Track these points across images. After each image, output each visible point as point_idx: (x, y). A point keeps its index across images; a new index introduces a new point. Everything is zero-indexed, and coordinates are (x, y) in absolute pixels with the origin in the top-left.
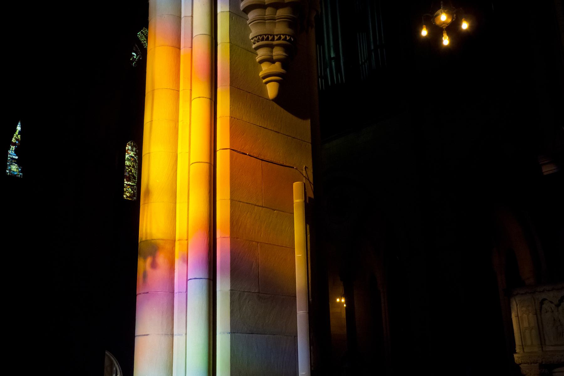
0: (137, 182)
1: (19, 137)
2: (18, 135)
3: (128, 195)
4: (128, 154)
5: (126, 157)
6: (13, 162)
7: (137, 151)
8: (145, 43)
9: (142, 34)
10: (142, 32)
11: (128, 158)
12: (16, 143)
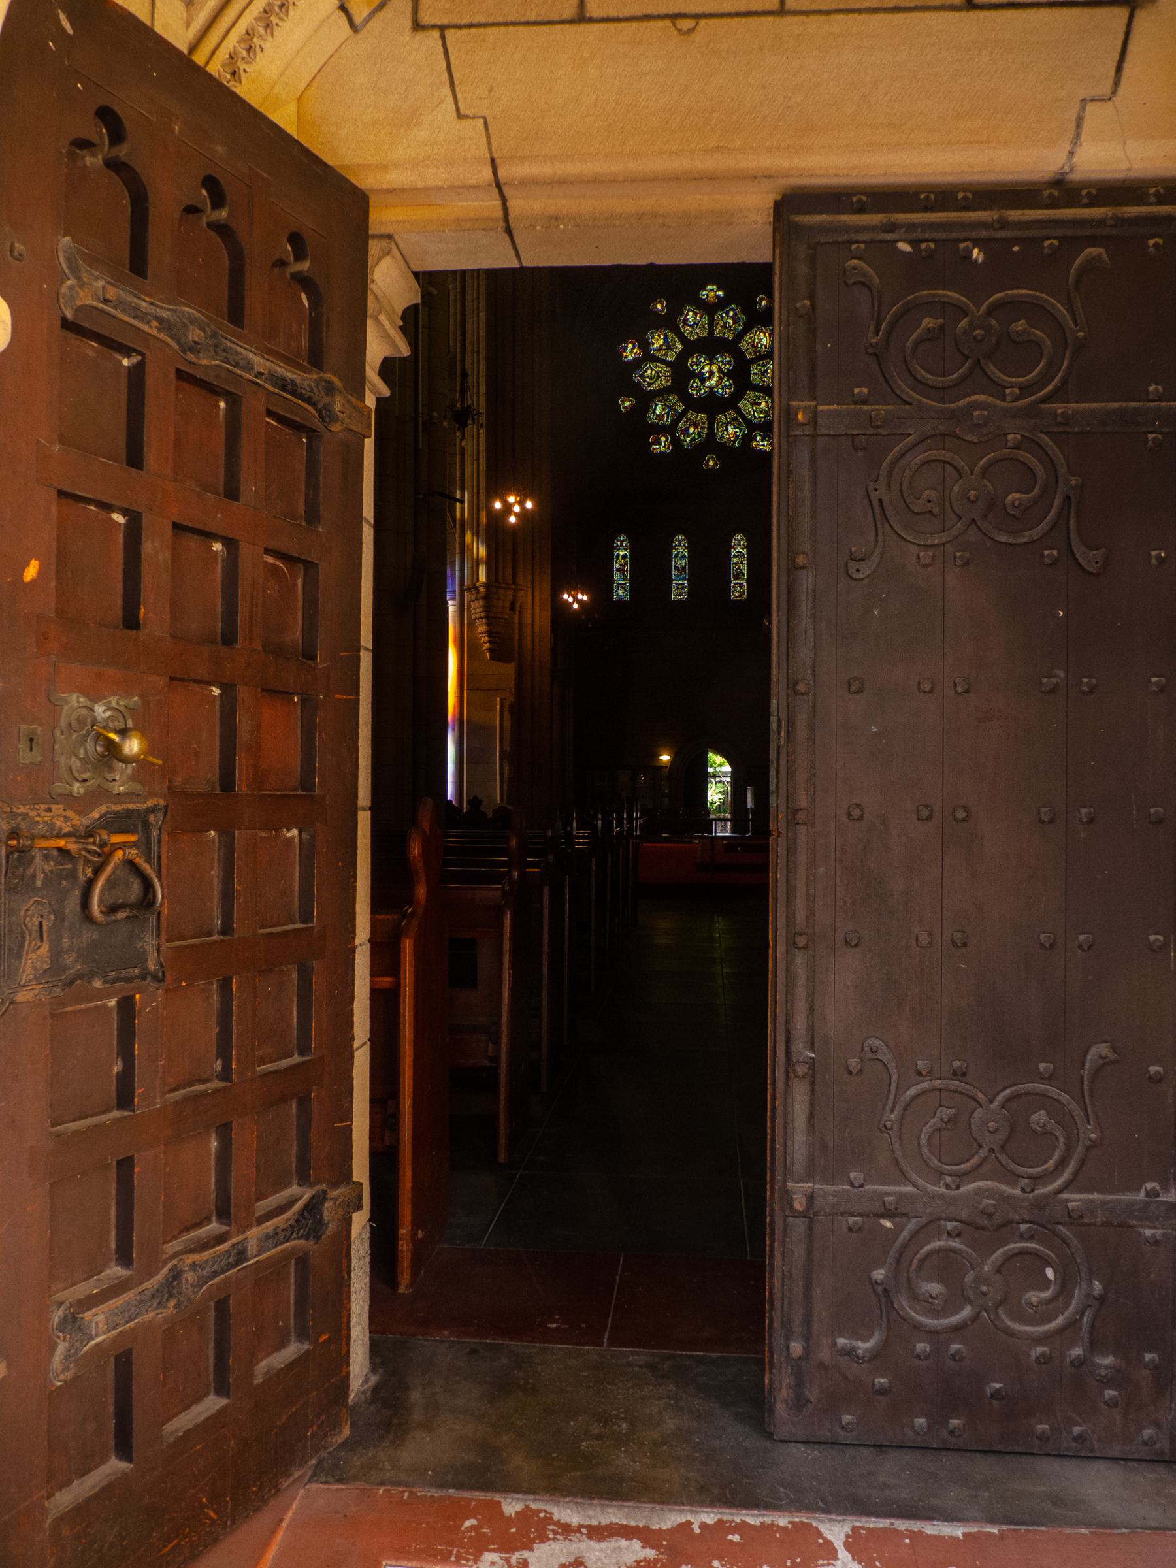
3: (737, 594)
10: (746, 399)
11: (734, 555)
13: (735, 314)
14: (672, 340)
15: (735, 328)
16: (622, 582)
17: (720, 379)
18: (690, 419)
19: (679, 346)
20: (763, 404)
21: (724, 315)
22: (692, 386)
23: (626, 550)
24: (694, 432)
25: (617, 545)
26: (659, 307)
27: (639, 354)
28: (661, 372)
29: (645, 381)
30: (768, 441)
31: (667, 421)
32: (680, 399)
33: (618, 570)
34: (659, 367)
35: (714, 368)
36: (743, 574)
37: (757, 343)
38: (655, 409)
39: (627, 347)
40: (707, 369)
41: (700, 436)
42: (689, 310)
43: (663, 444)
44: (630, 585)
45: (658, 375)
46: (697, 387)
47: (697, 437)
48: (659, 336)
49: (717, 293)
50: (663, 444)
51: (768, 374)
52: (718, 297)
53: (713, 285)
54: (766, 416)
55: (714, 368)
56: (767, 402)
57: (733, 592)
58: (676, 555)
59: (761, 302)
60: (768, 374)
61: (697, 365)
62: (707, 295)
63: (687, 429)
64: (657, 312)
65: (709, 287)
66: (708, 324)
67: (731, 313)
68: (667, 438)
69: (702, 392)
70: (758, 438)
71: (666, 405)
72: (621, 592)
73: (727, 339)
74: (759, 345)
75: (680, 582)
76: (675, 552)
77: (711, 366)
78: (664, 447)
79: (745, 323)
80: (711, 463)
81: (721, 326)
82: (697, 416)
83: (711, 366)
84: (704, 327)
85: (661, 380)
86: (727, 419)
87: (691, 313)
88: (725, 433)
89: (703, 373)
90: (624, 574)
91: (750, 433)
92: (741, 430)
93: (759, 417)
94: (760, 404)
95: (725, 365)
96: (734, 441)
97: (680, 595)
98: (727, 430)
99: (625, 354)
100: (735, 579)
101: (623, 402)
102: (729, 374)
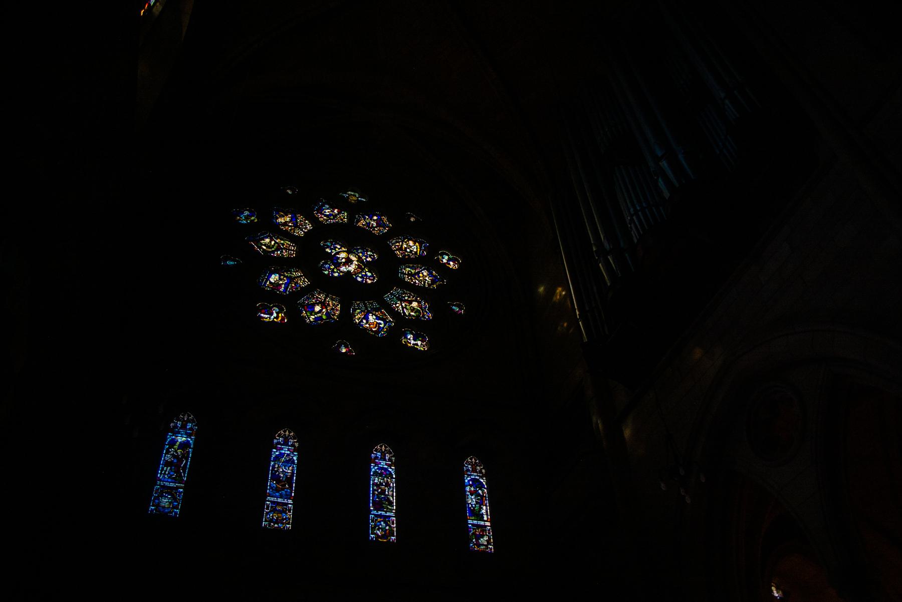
0: (395, 510)
5: (373, 470)
6: (166, 493)
7: (393, 459)
8: (398, 307)
10: (392, 294)
11: (376, 474)
12: (172, 461)
14: (300, 221)
16: (172, 485)
19: (309, 227)
20: (415, 304)
23: (189, 435)
24: (320, 312)
28: (283, 244)
29: (260, 248)
30: (422, 341)
33: (167, 464)
36: (391, 503)
37: (406, 248)
43: (275, 315)
44: (185, 492)
47: (324, 317)
56: (419, 302)
57: (373, 529)
58: (277, 458)
60: (419, 277)
63: (313, 305)
65: (349, 193)
70: (410, 336)
72: (165, 502)
74: (408, 250)
75: (280, 500)
76: (275, 453)
78: (277, 317)
88: (364, 321)
90: (177, 472)
94: (410, 302)
95: (367, 257)
97: (277, 522)
98: (367, 318)
102: (371, 266)
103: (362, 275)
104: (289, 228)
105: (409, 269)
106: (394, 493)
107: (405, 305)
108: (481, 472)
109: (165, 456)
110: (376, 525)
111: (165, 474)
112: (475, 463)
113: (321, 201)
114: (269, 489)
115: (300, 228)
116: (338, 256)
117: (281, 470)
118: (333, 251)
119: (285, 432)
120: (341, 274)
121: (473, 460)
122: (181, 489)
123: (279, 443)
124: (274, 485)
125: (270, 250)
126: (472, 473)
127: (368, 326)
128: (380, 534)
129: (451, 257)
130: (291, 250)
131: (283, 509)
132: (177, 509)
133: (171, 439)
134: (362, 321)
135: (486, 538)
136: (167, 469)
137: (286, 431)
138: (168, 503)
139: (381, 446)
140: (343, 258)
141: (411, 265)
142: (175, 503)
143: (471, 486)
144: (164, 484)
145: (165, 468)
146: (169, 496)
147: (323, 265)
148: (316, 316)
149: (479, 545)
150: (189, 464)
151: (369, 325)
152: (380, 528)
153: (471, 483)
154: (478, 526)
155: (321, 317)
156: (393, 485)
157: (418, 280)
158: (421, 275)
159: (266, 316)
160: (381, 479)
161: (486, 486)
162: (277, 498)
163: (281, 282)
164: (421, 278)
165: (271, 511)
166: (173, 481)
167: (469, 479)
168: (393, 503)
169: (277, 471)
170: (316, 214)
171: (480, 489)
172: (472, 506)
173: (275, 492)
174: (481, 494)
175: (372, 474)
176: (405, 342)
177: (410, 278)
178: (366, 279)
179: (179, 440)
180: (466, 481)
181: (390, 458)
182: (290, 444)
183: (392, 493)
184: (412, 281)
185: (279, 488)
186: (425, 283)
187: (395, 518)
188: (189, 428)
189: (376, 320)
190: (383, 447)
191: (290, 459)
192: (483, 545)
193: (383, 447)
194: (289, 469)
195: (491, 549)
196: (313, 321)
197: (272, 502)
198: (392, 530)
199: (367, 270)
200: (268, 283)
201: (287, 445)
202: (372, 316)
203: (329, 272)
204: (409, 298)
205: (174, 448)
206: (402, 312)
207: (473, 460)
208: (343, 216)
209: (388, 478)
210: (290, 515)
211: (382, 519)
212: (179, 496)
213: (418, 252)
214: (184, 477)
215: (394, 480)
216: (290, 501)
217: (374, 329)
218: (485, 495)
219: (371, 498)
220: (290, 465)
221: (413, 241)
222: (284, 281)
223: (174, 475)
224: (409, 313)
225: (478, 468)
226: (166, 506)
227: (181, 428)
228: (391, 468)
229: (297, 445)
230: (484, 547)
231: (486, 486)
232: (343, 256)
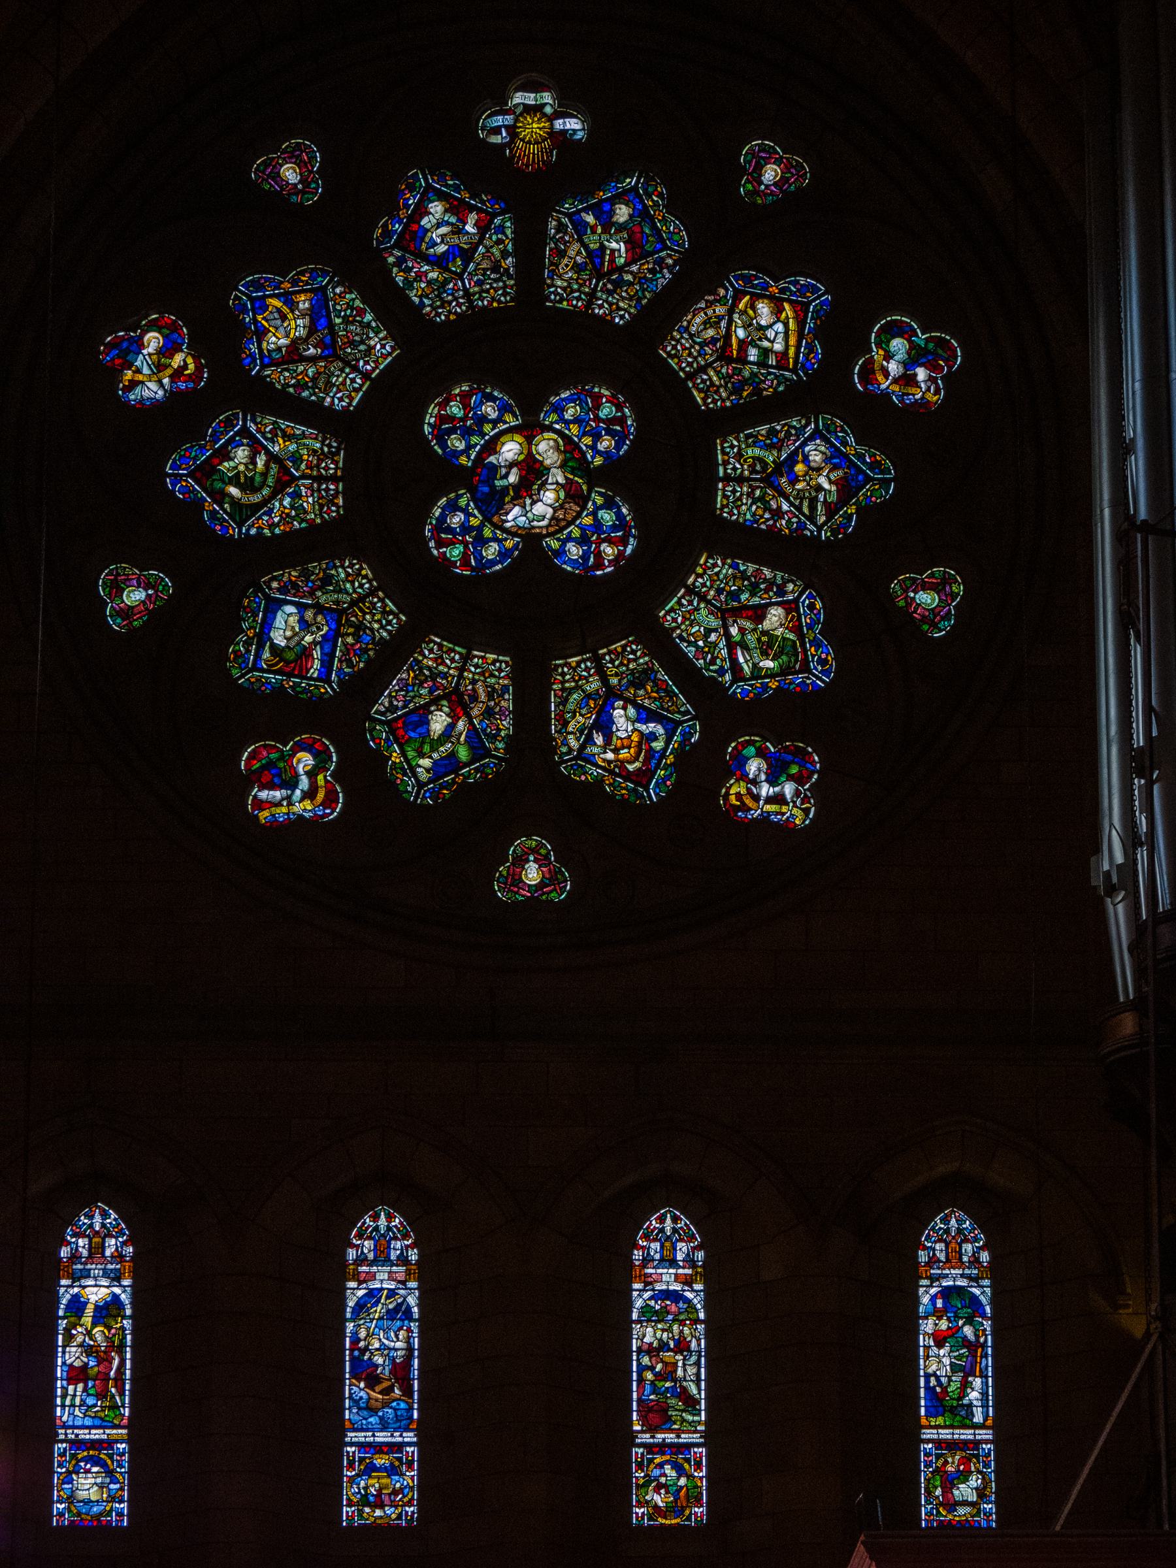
0: (706, 1423)
1: (99, 1338)
2: (95, 1324)
3: (659, 1500)
4: (647, 1284)
5: (639, 1303)
6: (84, 1459)
7: (700, 1255)
8: (715, 644)
9: (690, 603)
10: (691, 591)
12: (85, 1366)
13: (642, 214)
14: (346, 321)
15: (640, 279)
16: (97, 1434)
17: (573, 495)
18: (434, 676)
20: (775, 617)
21: (590, 219)
22: (441, 526)
23: (117, 1278)
25: (75, 1257)
26: (290, 174)
27: (196, 376)
28: (296, 459)
29: (220, 496)
30: (799, 779)
31: (325, 677)
32: (386, 583)
33: (77, 1375)
34: (287, 437)
35: (546, 448)
36: (690, 1403)
37: (744, 345)
38: (267, 625)
39: (140, 345)
40: (510, 449)
41: (478, 749)
42: (429, 194)
43: (304, 783)
45: (284, 470)
46: (465, 528)
47: (463, 754)
48: (288, 299)
49: (559, 124)
50: (304, 783)
51: (794, 480)
52: (561, 139)
53: (535, 88)
54: (784, 671)
55: (546, 448)
56: (790, 607)
58: (360, 1306)
59: (759, 168)
61: (466, 433)
62: (512, 130)
63: (421, 716)
64: (281, 197)
65: (519, 98)
66: (515, 254)
67: (622, 213)
68: (321, 757)
69: (491, 551)
70: (754, 767)
71: (319, 608)
73: (604, 322)
74: (753, 354)
75: (382, 1437)
76: (355, 1293)
77: (529, 440)
78: (310, 795)
79: (685, 259)
80: (532, 874)
81: (578, 268)
82: (466, 658)
83: (529, 440)
84: (496, 268)
85: (296, 495)
86: (604, 679)
87: (437, 208)
88: (599, 740)
89: (494, 468)
90: (102, 1395)
91: (715, 737)
92: (671, 727)
93: (757, 672)
94: (758, 614)
95: (597, 437)
96: (642, 778)
98: (604, 725)
99: (129, 375)
100: (652, 1429)
101: (117, 589)
103: (582, 528)
104: (310, 372)
105: (757, 452)
106: (703, 1370)
107: (742, 630)
108: (975, 1261)
109: (64, 1352)
110: (649, 1480)
111: (73, 1405)
112: (960, 1231)
113: (411, 188)
114: (350, 1409)
115: (347, 363)
116: (492, 459)
117: (377, 1345)
118: (474, 439)
119: (376, 1218)
120: (509, 544)
121: (953, 1222)
122: (121, 1443)
123: (361, 1260)
124: (362, 1394)
125: (256, 498)
126: (947, 1271)
127: (610, 756)
128: (661, 1504)
129: (921, 337)
130: (327, 479)
131: (392, 1464)
132: (121, 1502)
133: (68, 1296)
134: (589, 740)
135: (975, 1481)
136: (75, 1390)
137: (379, 1217)
138: (95, 1488)
139: (661, 1220)
140: (511, 465)
141: (763, 429)
142: (112, 1486)
143: (938, 1314)
144: (77, 1435)
145: (71, 1388)
146: (95, 1469)
147: (442, 519)
148: (435, 756)
149: (951, 1505)
150: (128, 1364)
151: (616, 751)
152: (665, 1486)
153: (939, 1303)
154: (953, 1446)
155: (452, 755)
156: (699, 1345)
157: (787, 499)
158: (800, 468)
159: (278, 794)
160: (663, 1330)
161: (988, 1309)
162: (373, 1430)
163: (309, 639)
164: (799, 486)
165: (358, 1475)
166: (97, 1422)
167: (933, 1291)
168: (699, 1403)
169: (366, 1349)
170: (400, 262)
171: (970, 1321)
172: (940, 1384)
173: (365, 1413)
174: (971, 1337)
175: (635, 1316)
176: (739, 796)
177: (758, 493)
178: (599, 542)
179: (93, 1298)
180: (925, 1300)
181: (688, 1255)
182: (394, 1255)
183: (694, 1371)
184: (767, 508)
185: (377, 1400)
186: (813, 502)
187: (703, 1450)
188: (112, 1256)
189: (638, 725)
190: (668, 1221)
191: (399, 1305)
192: (965, 1503)
193: (668, 1221)
194: (397, 1336)
195: (988, 1514)
196: (430, 781)
197: (361, 1446)
198: (696, 1487)
199: (599, 501)
200: (266, 655)
201: (387, 1261)
202: (624, 708)
203: (465, 544)
204: (753, 595)
205: (81, 1326)
206: (727, 665)
207: (953, 1222)
208: (499, 242)
209: (682, 1323)
210: (410, 1477)
211: (668, 1457)
212: (122, 1467)
213: (792, 351)
214: (123, 1406)
215: (701, 1327)
216: (410, 1437)
217: (631, 767)
218: (982, 1340)
219: (635, 1395)
220: (399, 1323)
221: (771, 298)
222: (319, 629)
223: (95, 1406)
224: (755, 665)
225: (968, 1248)
226: (93, 1498)
227: (91, 1256)
228: (693, 1290)
229: (413, 1255)
230: (968, 1509)
231: (988, 1309)
232: (510, 456)
